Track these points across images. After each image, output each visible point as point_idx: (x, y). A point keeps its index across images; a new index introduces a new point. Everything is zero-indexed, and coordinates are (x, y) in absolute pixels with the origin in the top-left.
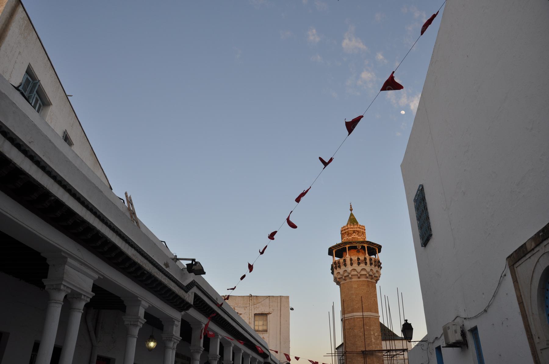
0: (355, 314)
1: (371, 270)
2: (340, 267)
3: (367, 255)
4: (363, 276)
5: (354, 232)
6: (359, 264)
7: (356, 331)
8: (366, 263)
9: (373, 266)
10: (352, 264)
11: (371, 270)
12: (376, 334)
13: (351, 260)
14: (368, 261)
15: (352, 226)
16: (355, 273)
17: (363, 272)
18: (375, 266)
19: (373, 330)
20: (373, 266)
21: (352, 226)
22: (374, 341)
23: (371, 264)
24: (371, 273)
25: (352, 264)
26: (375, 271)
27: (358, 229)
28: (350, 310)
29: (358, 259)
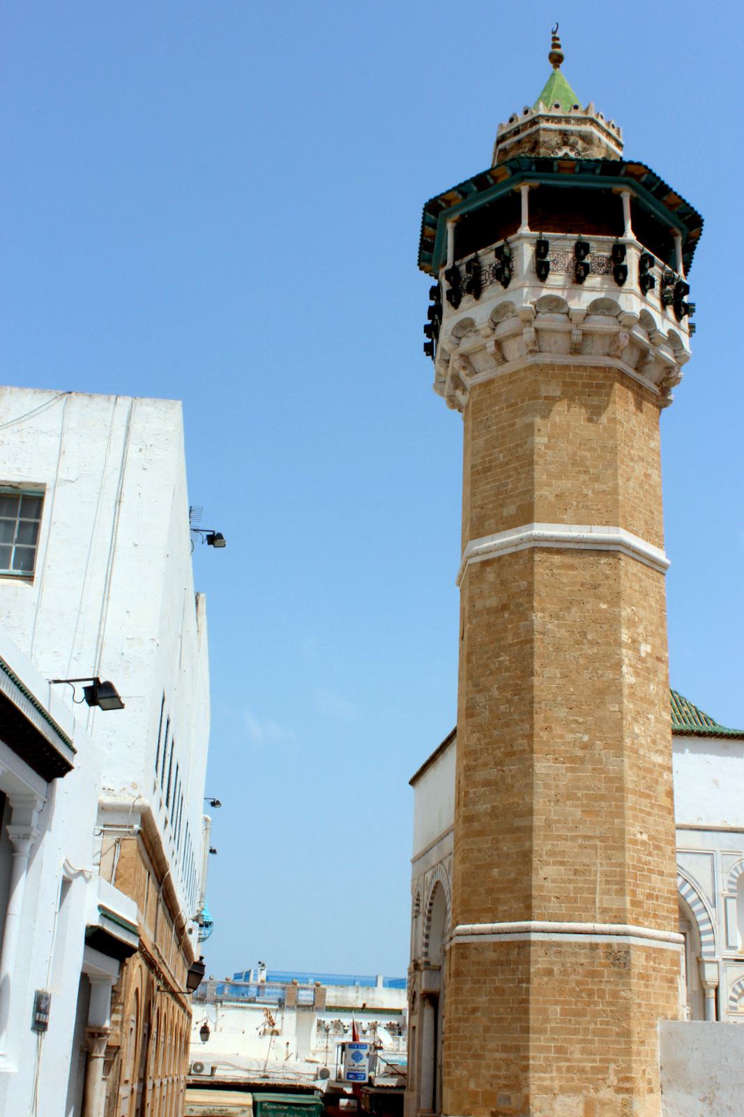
0: (541, 529)
3: (630, 235)
7: (538, 618)
10: (542, 270)
12: (645, 649)
13: (542, 249)
14: (632, 260)
18: (664, 303)
19: (632, 624)
20: (653, 297)
22: (629, 678)
23: (646, 283)
24: (640, 334)
25: (542, 270)
27: (587, 128)
28: (510, 510)
29: (581, 249)
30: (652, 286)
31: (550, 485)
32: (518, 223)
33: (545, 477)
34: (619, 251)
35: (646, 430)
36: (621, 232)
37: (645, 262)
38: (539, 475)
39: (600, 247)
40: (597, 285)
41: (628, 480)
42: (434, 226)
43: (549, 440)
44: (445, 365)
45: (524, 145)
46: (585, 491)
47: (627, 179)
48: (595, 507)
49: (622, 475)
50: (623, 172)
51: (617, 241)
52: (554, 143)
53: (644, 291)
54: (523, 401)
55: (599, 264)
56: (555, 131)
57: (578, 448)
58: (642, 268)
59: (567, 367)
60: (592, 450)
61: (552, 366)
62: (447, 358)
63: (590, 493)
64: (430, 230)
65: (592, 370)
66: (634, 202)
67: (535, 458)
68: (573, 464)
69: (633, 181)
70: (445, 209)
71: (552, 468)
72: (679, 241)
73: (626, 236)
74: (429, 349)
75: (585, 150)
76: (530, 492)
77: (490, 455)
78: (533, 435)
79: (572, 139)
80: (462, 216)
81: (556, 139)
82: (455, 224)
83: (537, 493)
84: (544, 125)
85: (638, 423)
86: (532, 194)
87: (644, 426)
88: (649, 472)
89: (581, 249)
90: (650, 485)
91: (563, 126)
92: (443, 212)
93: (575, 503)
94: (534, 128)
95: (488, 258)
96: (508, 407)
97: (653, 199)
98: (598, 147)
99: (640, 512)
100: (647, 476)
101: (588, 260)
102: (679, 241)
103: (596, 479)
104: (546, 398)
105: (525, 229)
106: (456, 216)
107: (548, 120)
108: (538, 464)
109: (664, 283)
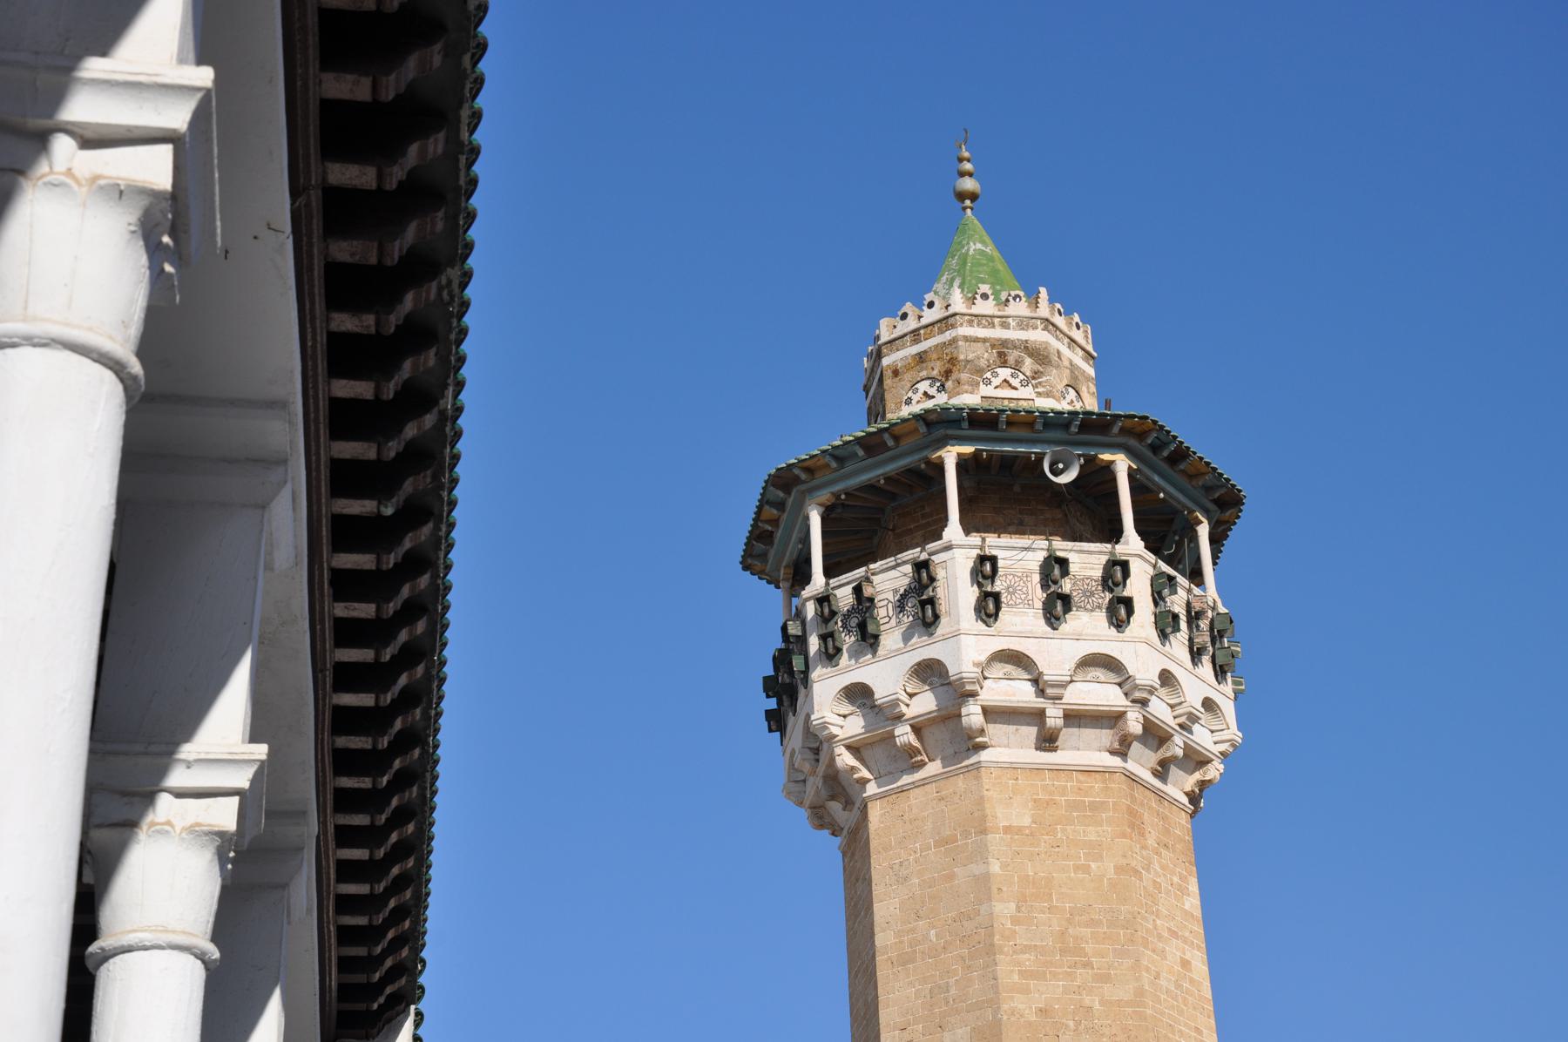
1: (1166, 678)
2: (869, 640)
3: (1132, 543)
4: (1089, 734)
5: (1002, 353)
6: (1057, 607)
8: (1120, 611)
9: (1179, 644)
10: (989, 607)
11: (1166, 678)
13: (985, 568)
14: (1138, 587)
15: (983, 307)
16: (1020, 693)
17: (1100, 693)
18: (1196, 654)
20: (1179, 644)
21: (983, 307)
23: (1165, 625)
24: (1159, 709)
25: (989, 607)
26: (1193, 699)
27: (1038, 336)
29: (1055, 566)
30: (1177, 629)
31: (1026, 991)
32: (943, 521)
33: (1016, 977)
34: (1117, 571)
35: (1176, 879)
36: (1113, 533)
37: (1161, 587)
38: (1007, 971)
39: (1086, 560)
40: (1088, 628)
41: (1157, 977)
42: (780, 506)
43: (1018, 909)
44: (812, 757)
45: (930, 365)
46: (1087, 1001)
47: (1121, 440)
48: (1107, 1031)
49: (1148, 970)
50: (1116, 430)
51: (1112, 553)
52: (983, 363)
53: (1163, 636)
54: (966, 834)
55: (1084, 592)
56: (985, 340)
57: (1069, 921)
58: (1157, 598)
59: (1039, 769)
60: (1093, 923)
61: (1013, 767)
62: (815, 745)
63: (1097, 1006)
64: (771, 512)
65: (1081, 777)
66: (1131, 475)
67: (997, 939)
68: (1063, 952)
69: (1133, 442)
70: (804, 482)
71: (1028, 959)
72: (1203, 531)
73: (1127, 543)
74: (776, 720)
75: (1037, 374)
76: (994, 1003)
77: (913, 930)
78: (990, 899)
79: (1012, 356)
80: (837, 496)
81: (986, 356)
82: (822, 509)
83: (1005, 1007)
84: (964, 331)
85: (1162, 868)
86: (963, 465)
87: (1173, 873)
88: (1188, 956)
89: (1055, 566)
90: (1192, 981)
91: (998, 333)
92: (803, 487)
93: (1071, 1023)
94: (948, 336)
95: (888, 580)
96: (938, 844)
97: (1164, 466)
98: (1058, 367)
99: (1181, 1033)
100: (1185, 964)
101: (1066, 586)
102: (1203, 531)
103: (1105, 978)
104: (1007, 830)
105: (953, 530)
106: (825, 496)
107: (970, 323)
108: (1002, 952)
109: (1194, 617)
